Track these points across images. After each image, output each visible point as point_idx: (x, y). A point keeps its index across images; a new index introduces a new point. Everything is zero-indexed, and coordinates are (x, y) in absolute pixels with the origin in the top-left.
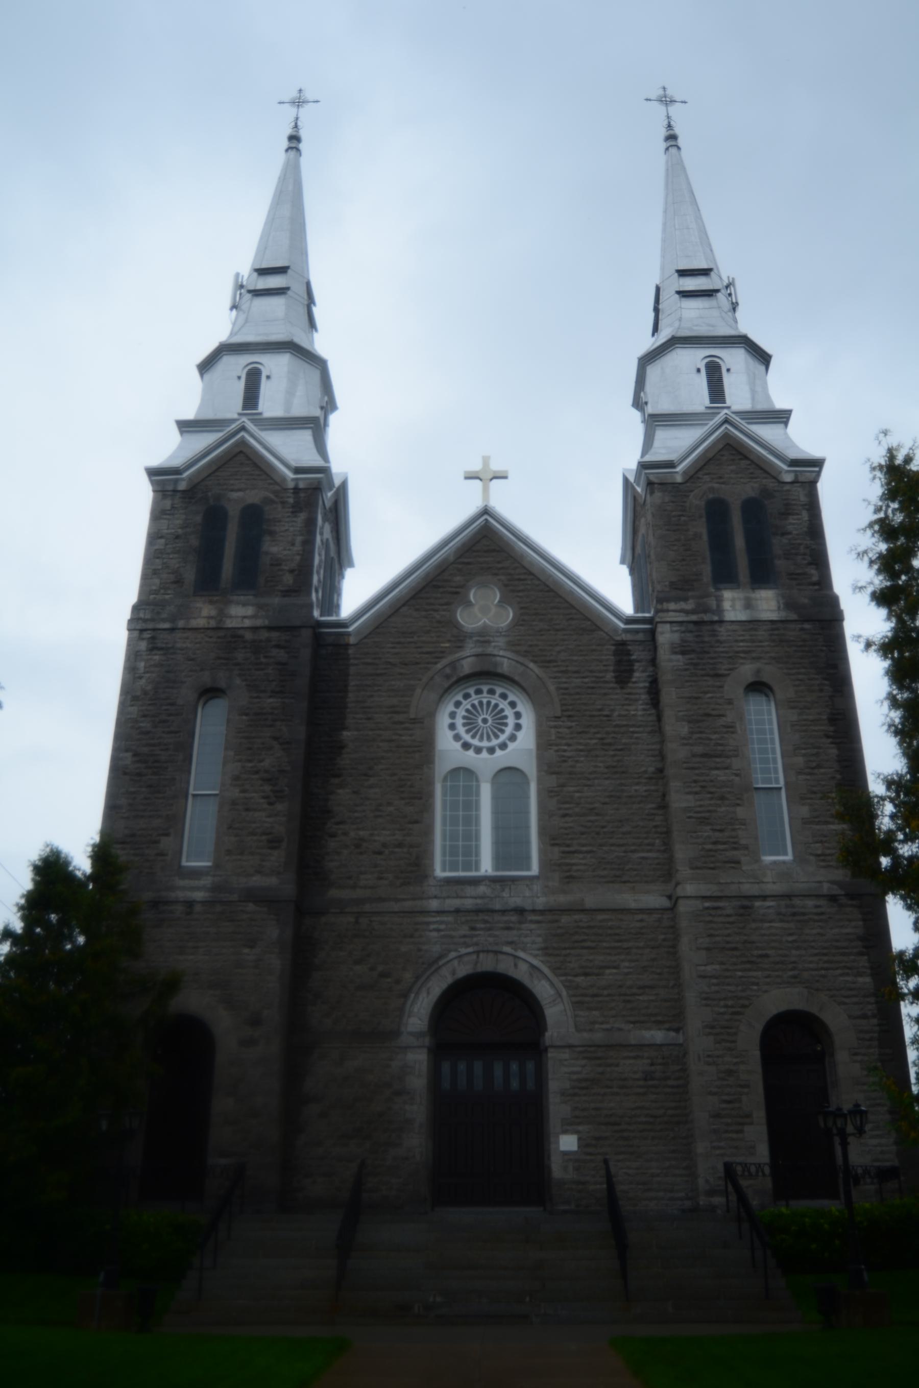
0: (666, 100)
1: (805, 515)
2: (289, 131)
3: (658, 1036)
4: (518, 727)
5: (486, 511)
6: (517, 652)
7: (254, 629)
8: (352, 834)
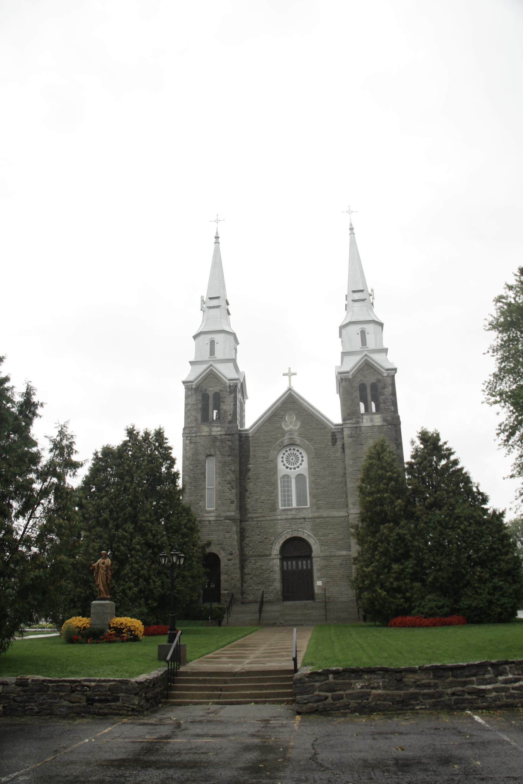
0: (350, 212)
1: (390, 388)
2: (215, 235)
3: (344, 553)
4: (302, 461)
5: (290, 389)
6: (301, 437)
7: (221, 435)
8: (254, 497)
